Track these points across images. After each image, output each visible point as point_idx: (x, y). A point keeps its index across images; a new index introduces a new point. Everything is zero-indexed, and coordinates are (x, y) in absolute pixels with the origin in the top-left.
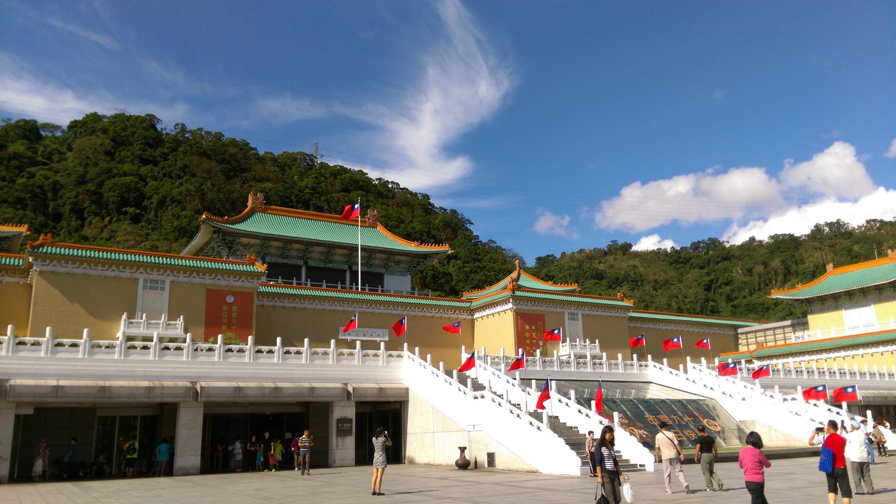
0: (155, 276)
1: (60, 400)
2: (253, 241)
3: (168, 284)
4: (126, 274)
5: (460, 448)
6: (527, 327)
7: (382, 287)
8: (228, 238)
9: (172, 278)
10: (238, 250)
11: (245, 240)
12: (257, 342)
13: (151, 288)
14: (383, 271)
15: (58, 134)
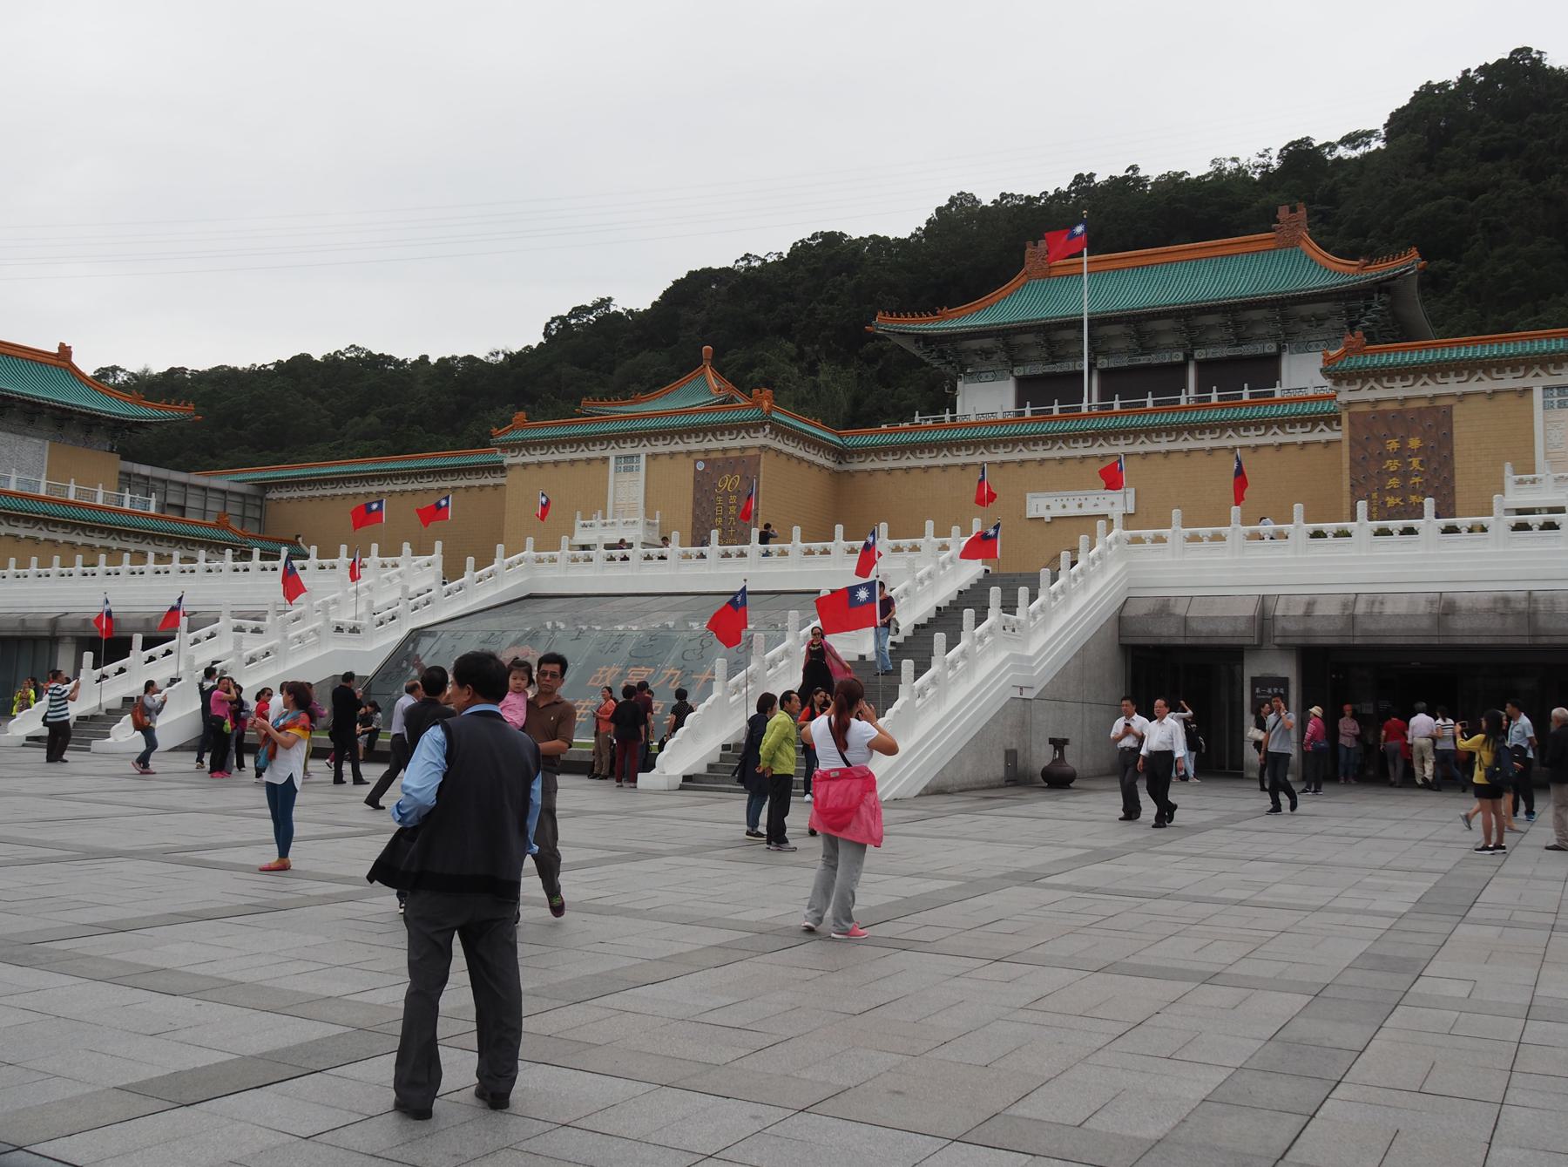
0: (628, 449)
1: (1215, 641)
2: (987, 343)
3: (643, 458)
4: (596, 452)
5: (1052, 741)
6: (1414, 443)
7: (953, 411)
8: (947, 347)
9: (650, 449)
10: (971, 366)
11: (975, 344)
12: (723, 541)
13: (626, 470)
14: (1270, 348)
15: (1377, 144)
